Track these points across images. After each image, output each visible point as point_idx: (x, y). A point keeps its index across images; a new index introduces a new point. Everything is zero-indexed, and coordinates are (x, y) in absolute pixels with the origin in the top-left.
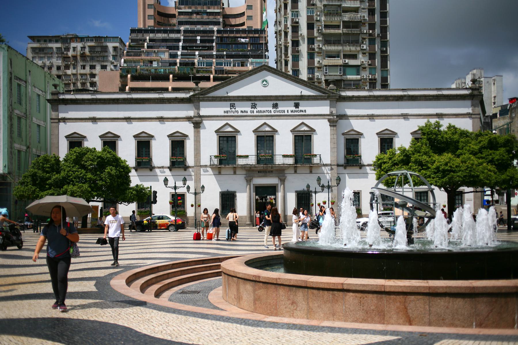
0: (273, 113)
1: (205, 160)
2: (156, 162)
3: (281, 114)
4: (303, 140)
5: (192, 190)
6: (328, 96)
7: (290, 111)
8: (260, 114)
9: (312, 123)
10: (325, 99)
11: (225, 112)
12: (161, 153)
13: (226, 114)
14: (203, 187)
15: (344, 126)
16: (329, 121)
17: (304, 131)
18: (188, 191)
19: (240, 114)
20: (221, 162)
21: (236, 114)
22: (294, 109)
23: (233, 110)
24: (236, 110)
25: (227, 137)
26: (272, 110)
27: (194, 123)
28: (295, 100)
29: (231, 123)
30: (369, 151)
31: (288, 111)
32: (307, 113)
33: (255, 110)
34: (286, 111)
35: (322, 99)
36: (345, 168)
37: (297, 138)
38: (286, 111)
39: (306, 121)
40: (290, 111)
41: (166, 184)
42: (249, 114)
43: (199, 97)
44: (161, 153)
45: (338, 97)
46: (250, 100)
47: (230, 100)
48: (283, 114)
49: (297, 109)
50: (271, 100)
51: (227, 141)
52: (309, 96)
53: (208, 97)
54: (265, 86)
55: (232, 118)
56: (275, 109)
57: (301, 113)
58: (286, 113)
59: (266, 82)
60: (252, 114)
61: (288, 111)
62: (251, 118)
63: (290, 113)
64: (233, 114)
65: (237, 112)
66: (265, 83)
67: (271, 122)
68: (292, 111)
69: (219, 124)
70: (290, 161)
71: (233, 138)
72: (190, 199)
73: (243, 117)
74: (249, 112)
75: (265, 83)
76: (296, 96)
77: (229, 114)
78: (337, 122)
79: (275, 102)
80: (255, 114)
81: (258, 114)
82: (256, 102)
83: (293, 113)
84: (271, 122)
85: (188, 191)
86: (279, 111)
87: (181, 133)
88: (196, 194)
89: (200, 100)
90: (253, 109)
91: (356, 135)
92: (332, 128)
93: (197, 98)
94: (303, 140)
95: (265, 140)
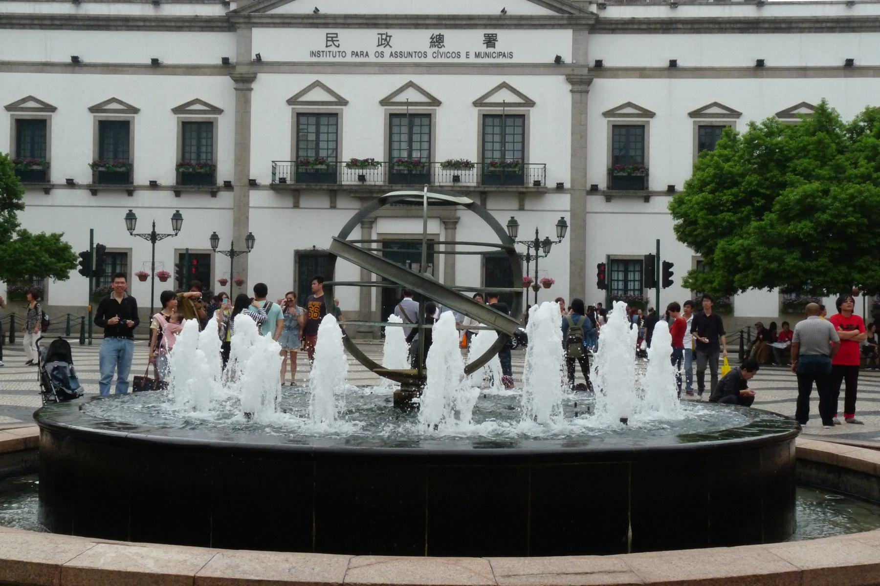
0: (430, 59)
1: (260, 171)
2: (141, 175)
3: (451, 60)
4: (504, 125)
5: (224, 245)
6: (569, 18)
7: (472, 55)
8: (399, 60)
9: (525, 84)
10: (561, 26)
11: (313, 54)
12: (155, 153)
13: (315, 59)
14: (250, 238)
15: (610, 93)
16: (570, 80)
17: (504, 104)
18: (214, 247)
19: (349, 59)
20: (299, 176)
21: (338, 59)
22: (483, 49)
23: (333, 49)
24: (341, 49)
25: (318, 115)
26: (430, 51)
27: (236, 80)
28: (486, 26)
29: (326, 79)
30: (672, 160)
31: (467, 54)
32: (515, 60)
33: (387, 51)
34: (463, 55)
35: (553, 26)
36: (609, 199)
37: (489, 121)
38: (463, 55)
39: (514, 81)
40: (472, 55)
41: (131, 229)
42: (372, 59)
43: (249, 17)
44: (155, 153)
45: (592, 22)
46: (375, 26)
47: (326, 25)
48: (456, 60)
49: (491, 50)
50: (427, 26)
51: (316, 125)
52: (521, 18)
53: (272, 17)
55: (330, 69)
56: (435, 49)
57: (501, 60)
58: (463, 60)
60: (380, 60)
61: (467, 54)
62: (377, 69)
63: (473, 60)
65: (343, 54)
67: (426, 81)
68: (478, 55)
69: (296, 83)
70: (470, 178)
71: (332, 120)
72: (221, 267)
73: (358, 67)
76: (490, 18)
77: (322, 59)
78: (589, 83)
79: (437, 32)
80: (387, 59)
81: (393, 60)
82: (390, 32)
83: (479, 61)
84: (426, 81)
85: (214, 247)
86: (446, 55)
87: (205, 104)
88: (232, 254)
89: (250, 23)
90: (381, 49)
91: (638, 116)
92: (578, 96)
93: (244, 17)
94: (504, 125)
95: (410, 123)
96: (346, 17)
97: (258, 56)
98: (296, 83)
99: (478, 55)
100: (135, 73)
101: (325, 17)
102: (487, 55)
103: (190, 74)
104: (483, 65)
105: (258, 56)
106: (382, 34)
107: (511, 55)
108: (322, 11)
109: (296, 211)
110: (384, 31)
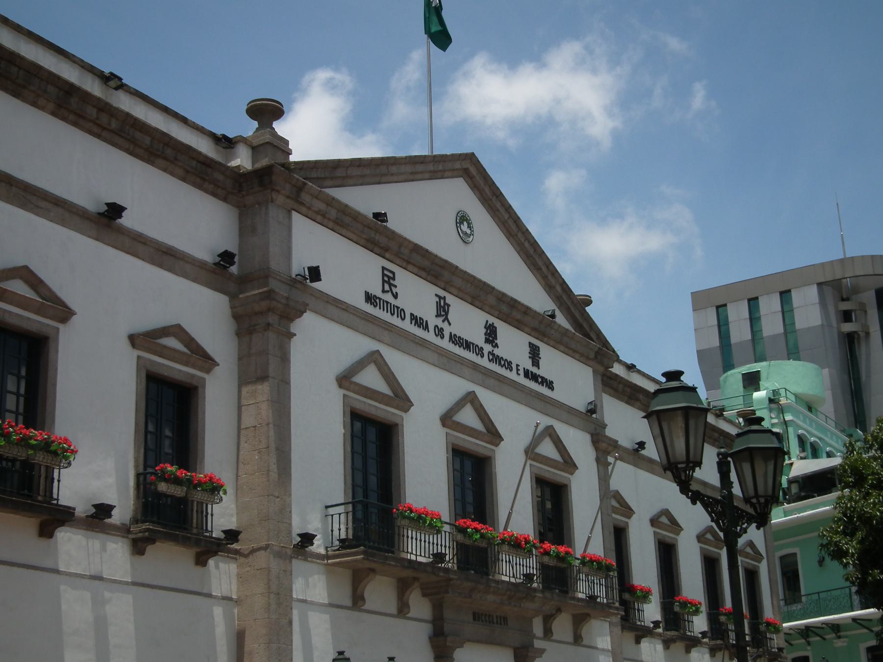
0: (484, 362)
7: (521, 372)
11: (370, 298)
13: (369, 308)
21: (395, 321)
22: (528, 364)
23: (388, 297)
26: (487, 348)
42: (430, 336)
53: (332, 202)
54: (465, 239)
58: (512, 375)
59: (469, 227)
60: (437, 341)
64: (385, 316)
65: (400, 313)
66: (465, 227)
68: (527, 374)
74: (431, 328)
75: (465, 227)
79: (492, 320)
80: (445, 344)
82: (450, 299)
90: (439, 322)
96: (417, 249)
97: (315, 273)
98: (350, 345)
99: (527, 374)
100: (63, 223)
101: (393, 235)
102: (534, 377)
103: (161, 266)
104: (531, 392)
105: (315, 273)
106: (440, 298)
107: (550, 385)
108: (393, 224)
109: (356, 614)
110: (442, 293)
